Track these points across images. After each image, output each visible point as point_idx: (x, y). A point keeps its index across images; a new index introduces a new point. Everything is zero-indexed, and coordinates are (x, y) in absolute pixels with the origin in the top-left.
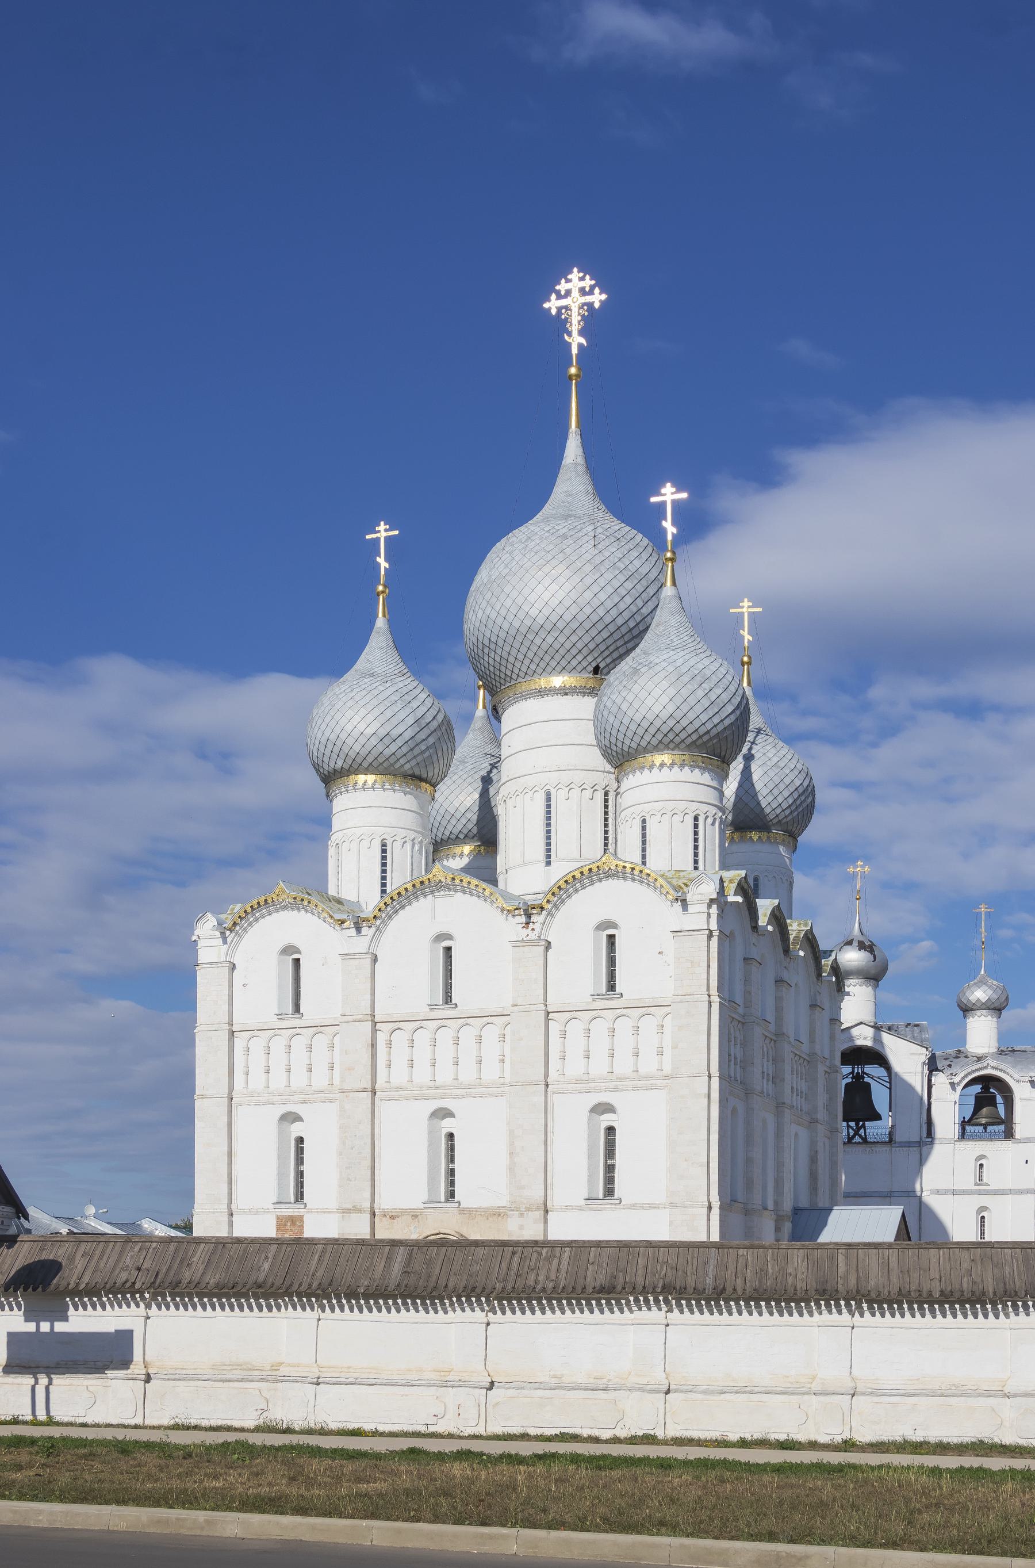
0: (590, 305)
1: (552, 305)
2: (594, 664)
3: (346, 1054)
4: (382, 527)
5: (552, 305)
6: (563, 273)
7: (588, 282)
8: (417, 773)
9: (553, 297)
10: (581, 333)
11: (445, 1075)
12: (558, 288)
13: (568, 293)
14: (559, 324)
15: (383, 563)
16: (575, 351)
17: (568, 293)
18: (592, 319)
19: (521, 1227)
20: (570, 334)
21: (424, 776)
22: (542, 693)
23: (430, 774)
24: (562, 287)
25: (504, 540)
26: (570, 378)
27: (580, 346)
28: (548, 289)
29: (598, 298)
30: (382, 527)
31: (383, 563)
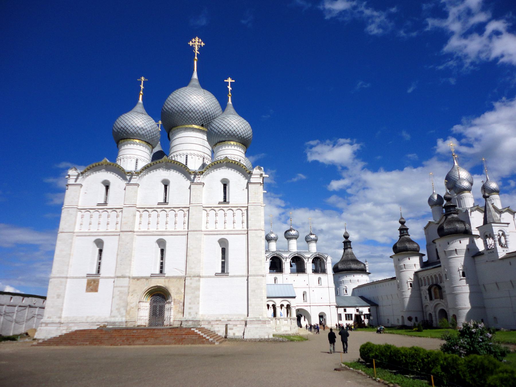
0: (201, 46)
1: (191, 43)
2: (202, 124)
3: (125, 218)
4: (143, 78)
5: (191, 43)
6: (195, 38)
7: (200, 40)
8: (149, 142)
9: (191, 42)
10: (198, 51)
11: (162, 228)
12: (192, 40)
13: (195, 42)
14: (193, 48)
15: (142, 87)
16: (196, 55)
17: (195, 42)
18: (201, 49)
19: (191, 284)
20: (195, 51)
21: (151, 143)
22: (186, 129)
23: (153, 143)
24: (194, 40)
25: (177, 90)
26: (195, 59)
27: (198, 54)
28: (190, 40)
29: (203, 44)
30: (143, 78)
31: (142, 87)
